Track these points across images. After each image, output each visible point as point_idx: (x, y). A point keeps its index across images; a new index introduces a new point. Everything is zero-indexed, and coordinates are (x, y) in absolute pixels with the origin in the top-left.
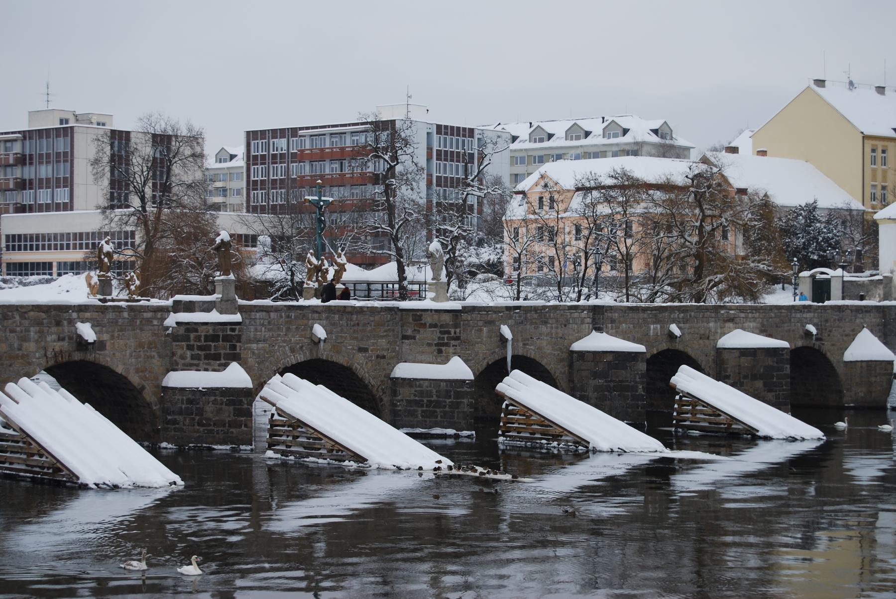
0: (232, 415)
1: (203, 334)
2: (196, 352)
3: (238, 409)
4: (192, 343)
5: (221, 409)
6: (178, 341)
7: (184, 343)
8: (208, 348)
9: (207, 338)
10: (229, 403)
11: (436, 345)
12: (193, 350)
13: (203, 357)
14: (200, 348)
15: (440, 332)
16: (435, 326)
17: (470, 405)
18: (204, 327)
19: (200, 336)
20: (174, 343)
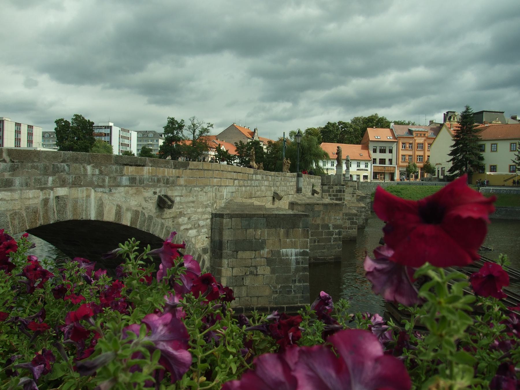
0: (349, 224)
1: (335, 189)
2: (332, 197)
3: (352, 221)
4: (330, 193)
5: (345, 222)
6: (325, 192)
7: (327, 193)
8: (337, 195)
9: (337, 191)
10: (349, 219)
11: (353, 193)
12: (331, 196)
13: (335, 199)
14: (334, 195)
15: (353, 189)
16: (351, 186)
17: (365, 216)
18: (336, 186)
19: (334, 190)
20: (323, 193)
